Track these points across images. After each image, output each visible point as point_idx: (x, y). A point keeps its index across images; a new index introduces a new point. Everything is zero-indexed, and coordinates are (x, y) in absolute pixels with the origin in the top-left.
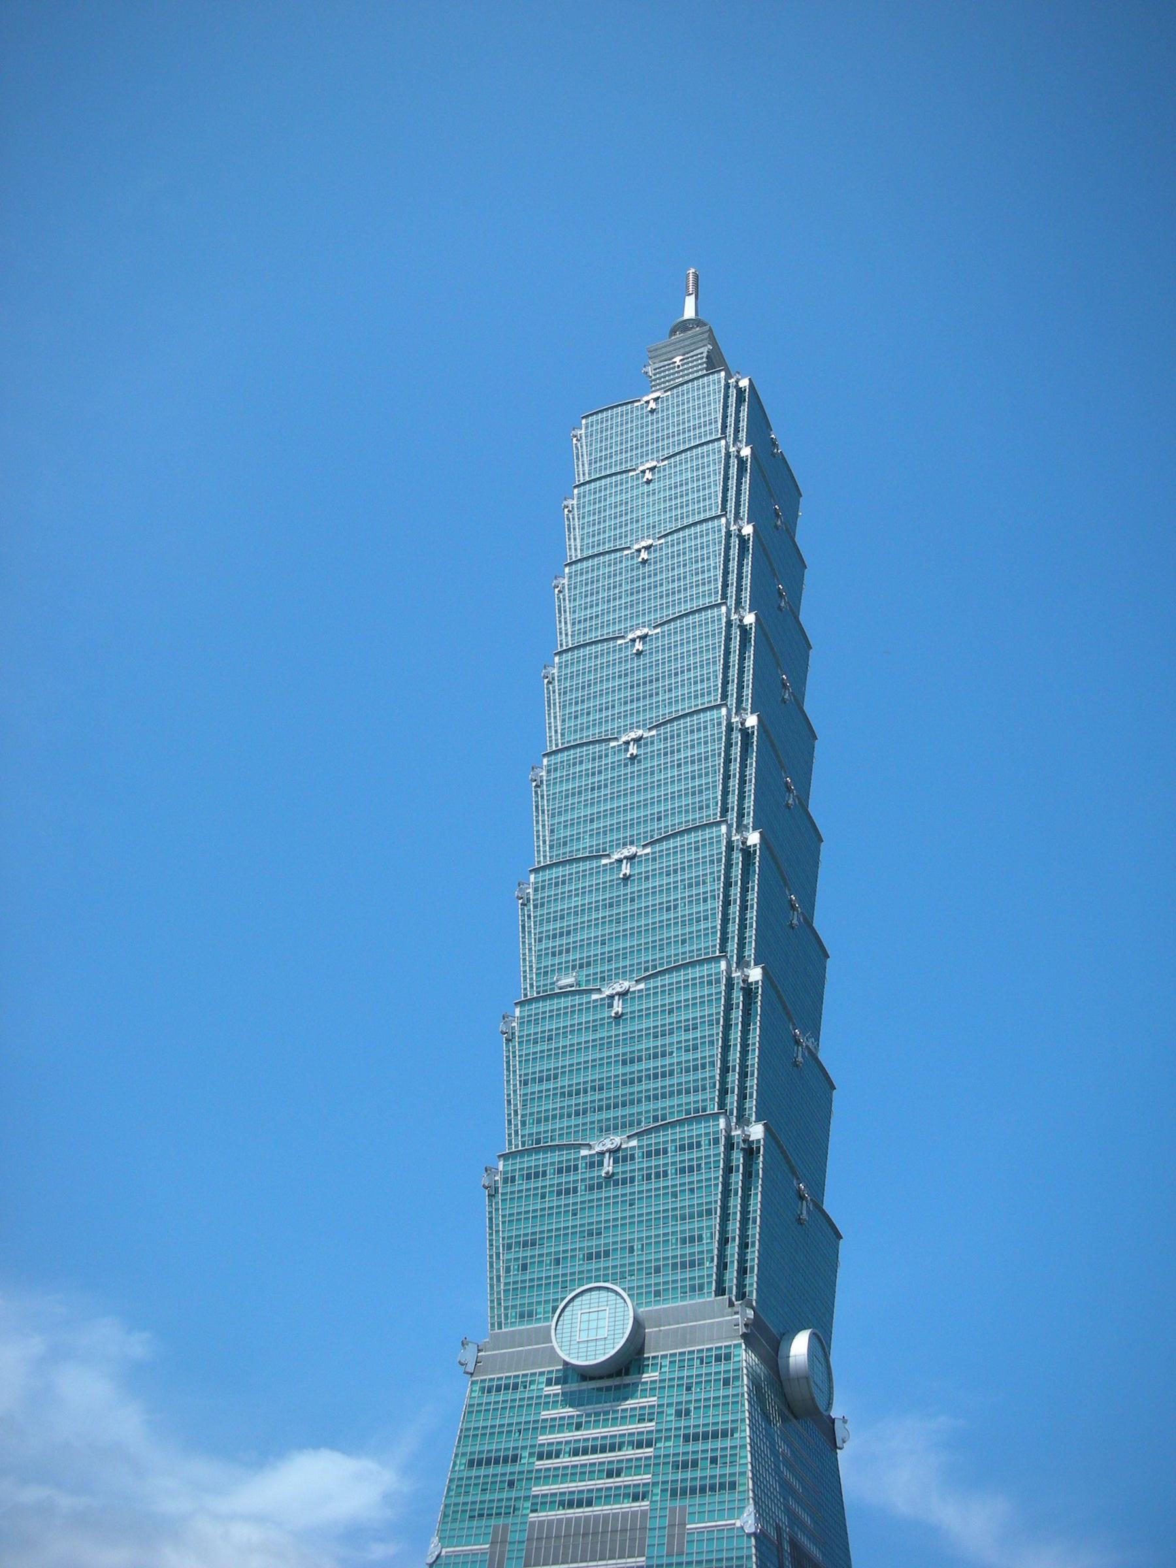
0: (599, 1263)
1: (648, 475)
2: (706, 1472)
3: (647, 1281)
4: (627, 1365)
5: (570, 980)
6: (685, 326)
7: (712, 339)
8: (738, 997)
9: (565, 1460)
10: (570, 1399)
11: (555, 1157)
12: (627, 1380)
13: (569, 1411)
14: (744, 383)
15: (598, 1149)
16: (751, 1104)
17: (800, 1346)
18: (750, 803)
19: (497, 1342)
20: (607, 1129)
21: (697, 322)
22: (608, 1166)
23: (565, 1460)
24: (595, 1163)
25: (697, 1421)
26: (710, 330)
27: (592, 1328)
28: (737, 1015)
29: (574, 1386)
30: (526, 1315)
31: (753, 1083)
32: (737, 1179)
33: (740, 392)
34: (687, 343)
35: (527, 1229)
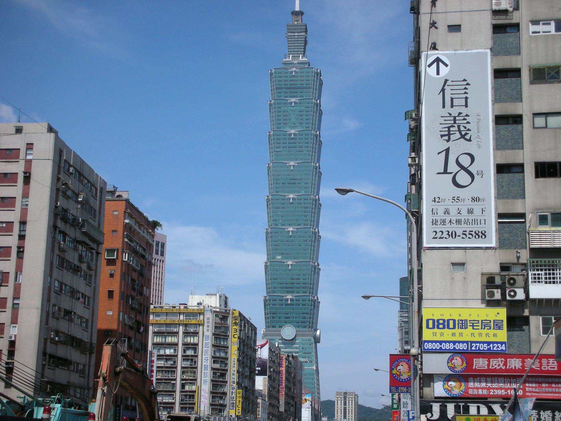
1: (293, 105)
7: (306, 31)
11: (279, 298)
12: (294, 341)
14: (319, 71)
15: (288, 297)
17: (318, 332)
20: (288, 292)
22: (289, 302)
24: (287, 300)
25: (306, 351)
26: (306, 26)
29: (284, 341)
30: (274, 327)
34: (299, 27)
35: (273, 311)
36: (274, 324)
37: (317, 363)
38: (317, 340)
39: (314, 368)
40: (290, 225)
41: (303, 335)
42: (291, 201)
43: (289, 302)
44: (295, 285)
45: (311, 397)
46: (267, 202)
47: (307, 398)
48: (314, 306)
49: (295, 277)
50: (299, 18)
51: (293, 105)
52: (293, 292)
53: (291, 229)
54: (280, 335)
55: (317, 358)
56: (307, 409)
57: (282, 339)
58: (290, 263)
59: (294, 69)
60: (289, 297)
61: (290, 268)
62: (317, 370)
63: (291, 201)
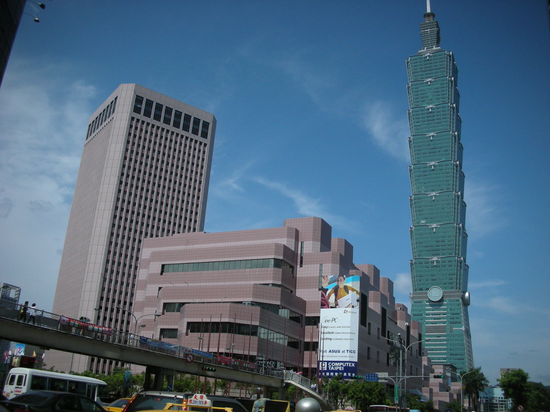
0: (435, 282)
2: (456, 320)
3: (443, 286)
4: (441, 300)
5: (423, 222)
6: (428, 15)
7: (438, 26)
8: (458, 231)
9: (431, 316)
10: (431, 305)
13: (430, 308)
14: (451, 53)
15: (433, 259)
16: (460, 252)
17: (467, 294)
18: (458, 183)
19: (417, 294)
20: (434, 255)
21: (432, 15)
22: (435, 264)
23: (431, 316)
24: (433, 262)
26: (437, 22)
27: (435, 294)
28: (458, 234)
29: (431, 303)
30: (421, 289)
31: (460, 247)
32: (459, 268)
33: (450, 57)
36: (420, 287)
37: (467, 325)
38: (466, 303)
39: (463, 328)
40: (433, 191)
41: (450, 296)
42: (433, 168)
43: (435, 264)
44: (440, 247)
45: (358, 283)
46: (410, 171)
47: (349, 284)
48: (461, 267)
49: (441, 239)
50: (431, 18)
51: (429, 83)
52: (439, 255)
53: (434, 194)
54: (427, 297)
55: (467, 320)
56: (349, 309)
57: (430, 301)
58: (434, 225)
59: (428, 54)
60: (435, 259)
61: (434, 231)
62: (468, 332)
63: (433, 168)
